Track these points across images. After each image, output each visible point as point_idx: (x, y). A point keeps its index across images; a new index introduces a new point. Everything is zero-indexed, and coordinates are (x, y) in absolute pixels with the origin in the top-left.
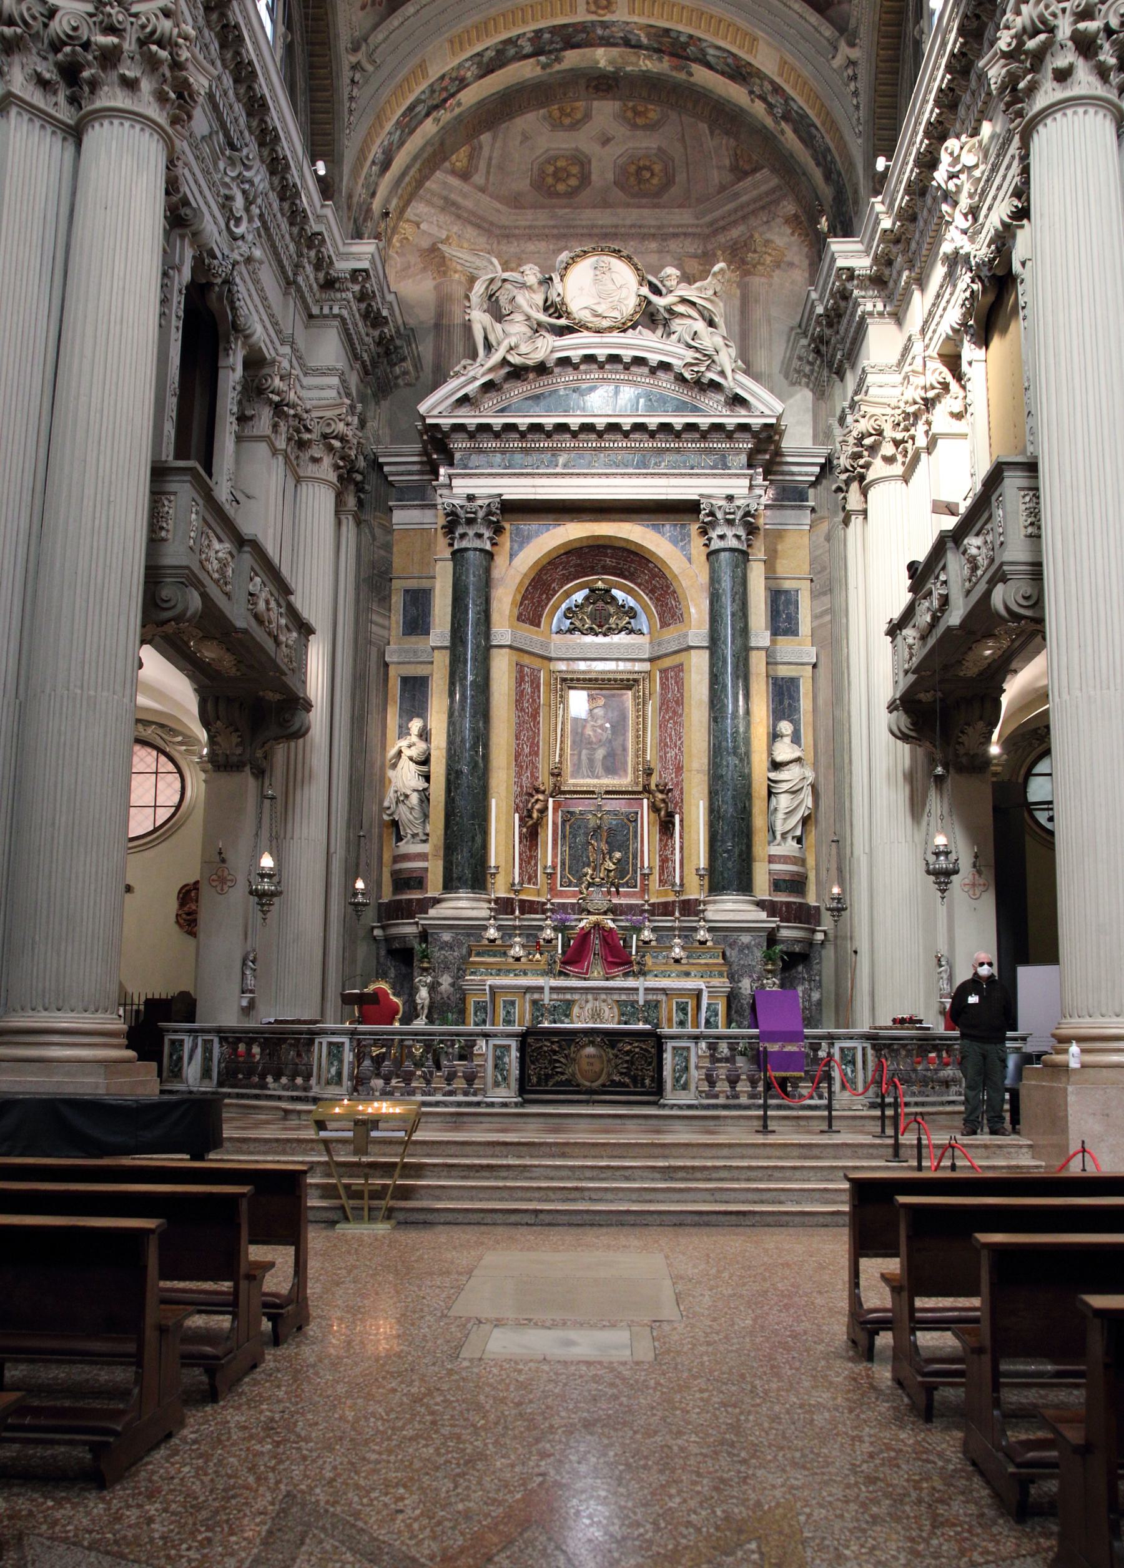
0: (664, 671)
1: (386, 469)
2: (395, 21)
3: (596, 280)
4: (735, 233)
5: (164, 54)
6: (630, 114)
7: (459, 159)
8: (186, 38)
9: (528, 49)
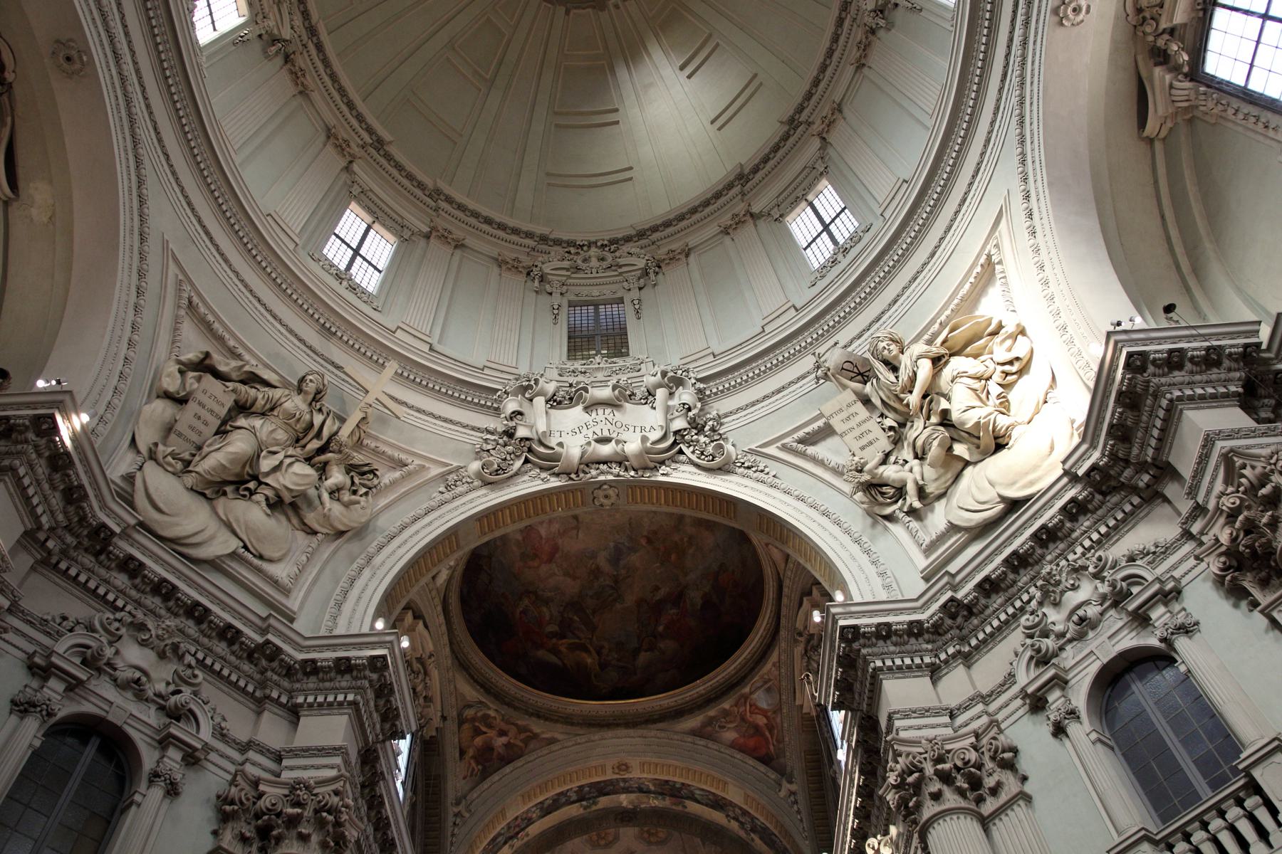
2: (486, 785)
5: (331, 818)
6: (646, 835)
8: (347, 807)
9: (574, 797)
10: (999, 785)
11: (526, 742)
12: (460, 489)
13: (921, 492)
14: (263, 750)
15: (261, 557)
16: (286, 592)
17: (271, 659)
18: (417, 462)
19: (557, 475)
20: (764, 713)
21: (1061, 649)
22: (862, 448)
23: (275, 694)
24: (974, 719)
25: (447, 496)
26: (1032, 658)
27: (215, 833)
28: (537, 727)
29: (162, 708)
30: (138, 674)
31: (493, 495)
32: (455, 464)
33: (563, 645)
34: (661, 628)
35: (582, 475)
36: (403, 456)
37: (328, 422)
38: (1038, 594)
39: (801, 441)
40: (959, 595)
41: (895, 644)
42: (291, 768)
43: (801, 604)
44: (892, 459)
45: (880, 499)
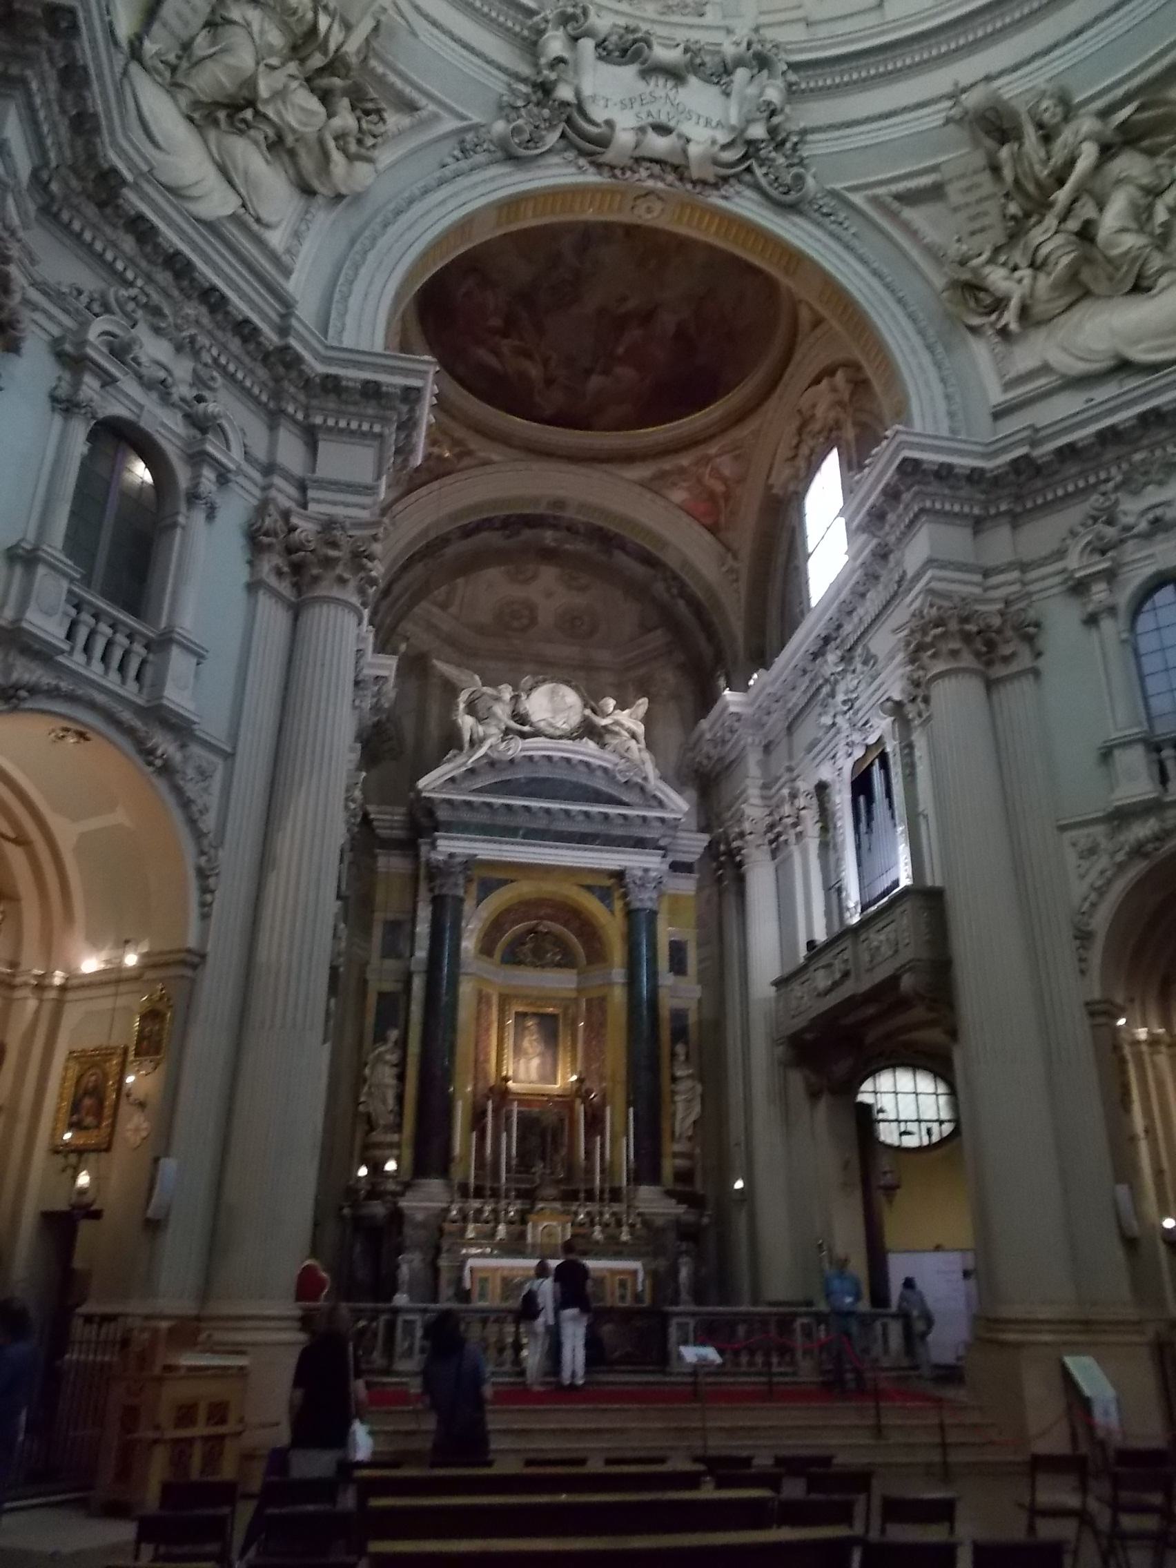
0: (589, 1001)
1: (375, 823)
3: (551, 699)
4: (642, 671)
7: (440, 593)
10: (1014, 655)
11: (460, 456)
12: (480, 158)
13: (1024, 312)
14: (287, 476)
15: (258, 220)
16: (287, 272)
17: (288, 366)
18: (432, 107)
19: (599, 166)
20: (724, 480)
21: (1122, 541)
22: (973, 233)
23: (291, 409)
24: (1007, 584)
25: (464, 164)
26: (1088, 543)
27: (251, 563)
28: (475, 442)
29: (187, 416)
30: (162, 374)
31: (519, 176)
32: (476, 119)
33: (506, 345)
34: (620, 350)
35: (628, 174)
36: (415, 95)
37: (336, 27)
38: (1119, 478)
39: (898, 197)
40: (1036, 453)
41: (951, 487)
42: (318, 501)
43: (817, 381)
44: (1002, 258)
45: (972, 304)
